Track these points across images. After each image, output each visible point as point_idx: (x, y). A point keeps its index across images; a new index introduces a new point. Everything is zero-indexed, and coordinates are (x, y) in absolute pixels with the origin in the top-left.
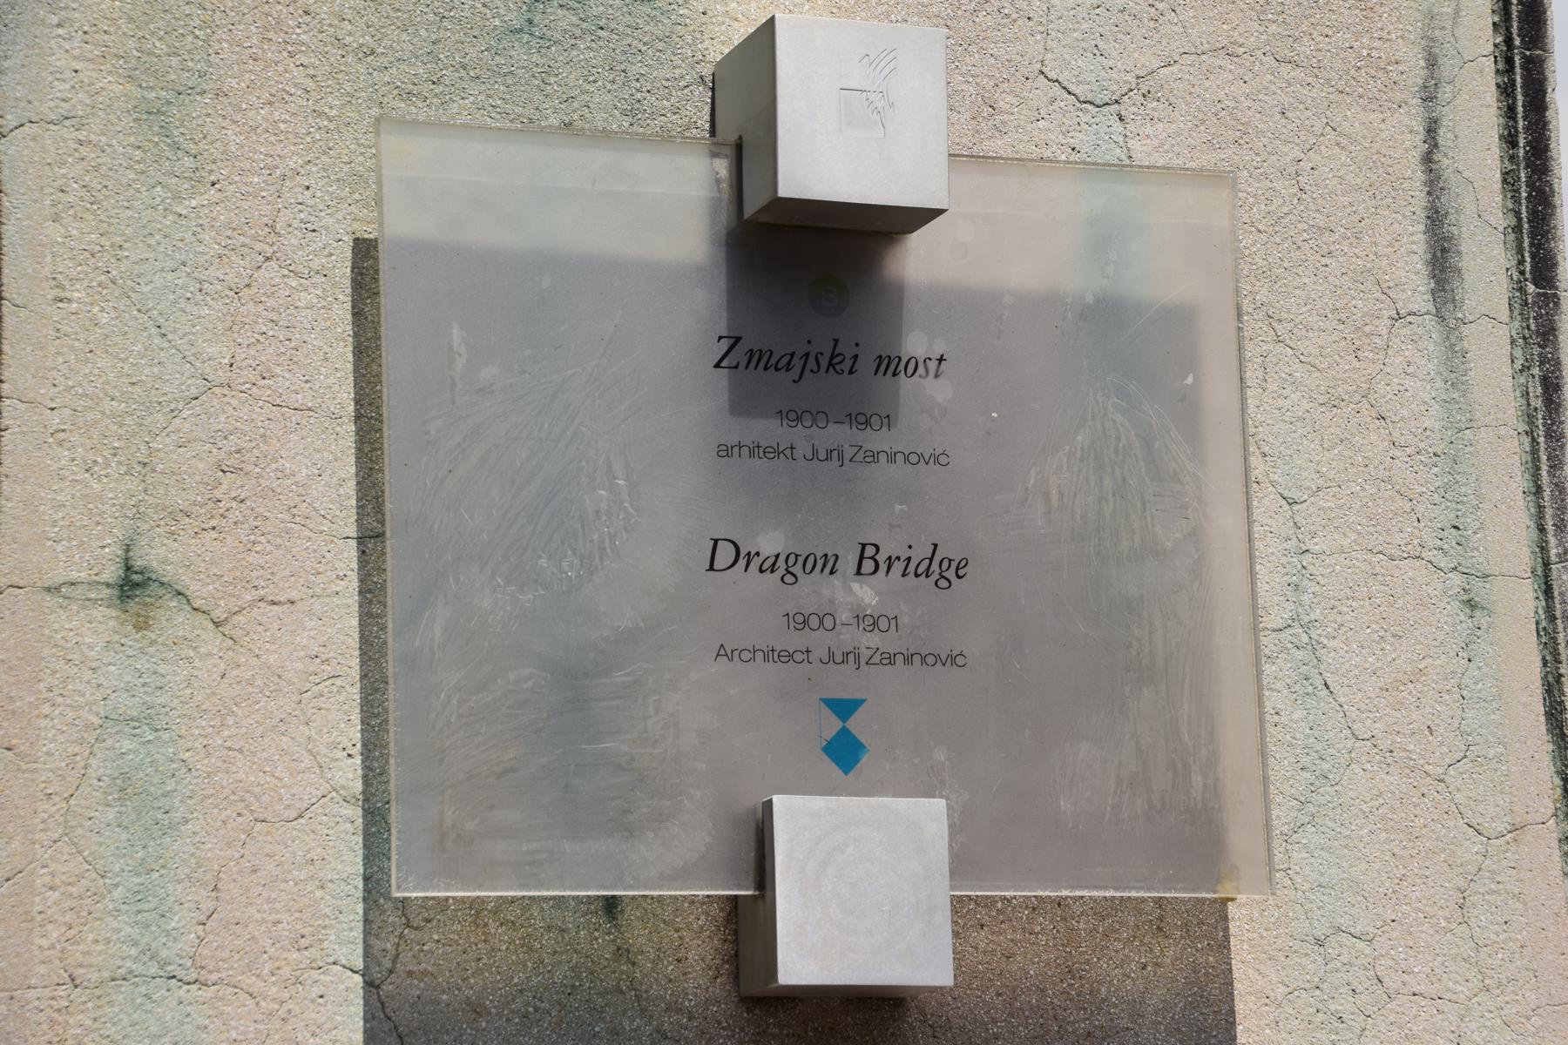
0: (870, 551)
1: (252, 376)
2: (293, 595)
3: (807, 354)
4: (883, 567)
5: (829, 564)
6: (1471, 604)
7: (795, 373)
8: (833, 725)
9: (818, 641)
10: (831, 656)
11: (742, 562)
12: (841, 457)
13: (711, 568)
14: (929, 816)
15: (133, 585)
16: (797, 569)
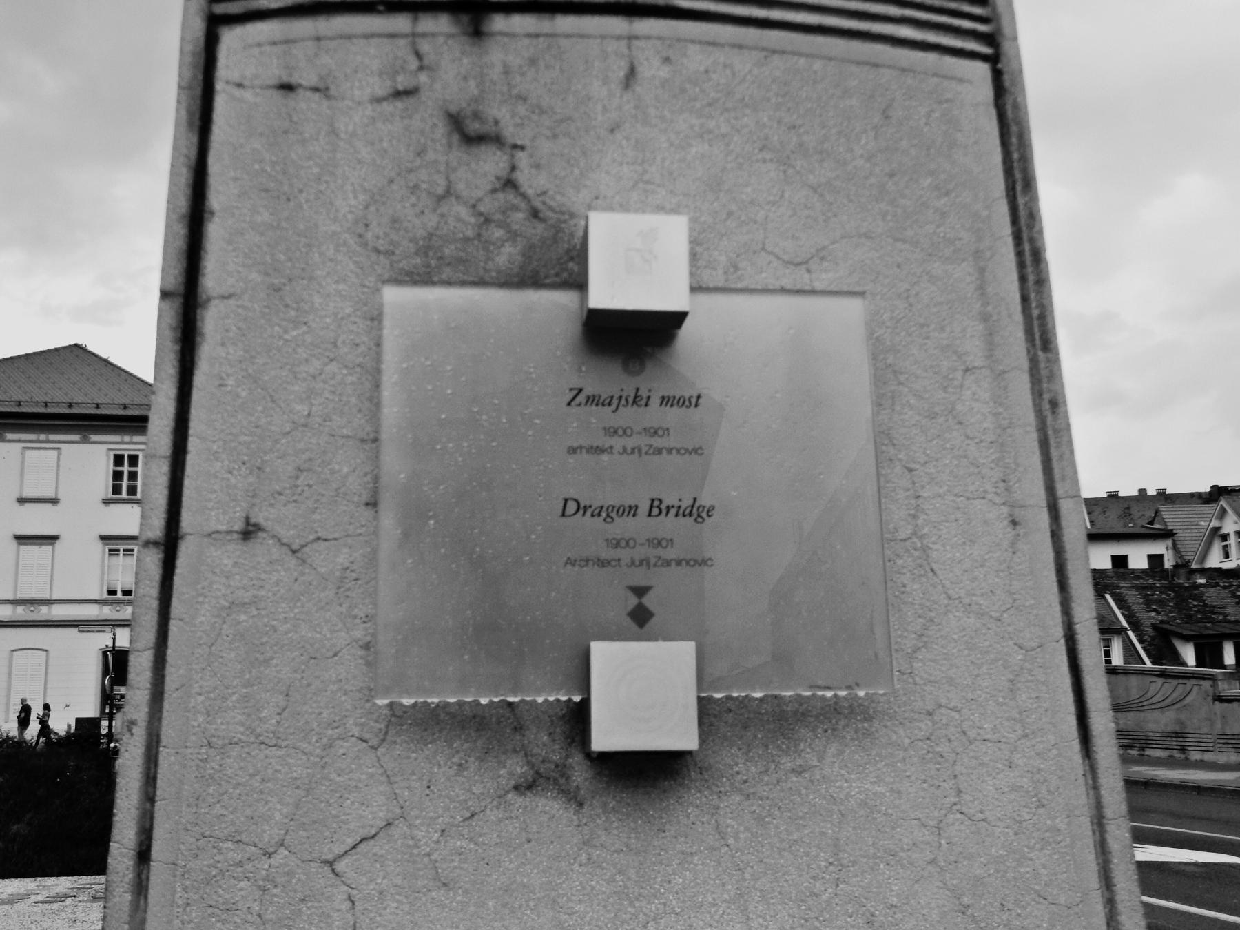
0: (656, 503)
1: (318, 420)
2: (336, 535)
3: (621, 397)
4: (664, 512)
5: (632, 510)
6: (1014, 523)
7: (614, 407)
8: (633, 601)
9: (624, 554)
10: (633, 563)
11: (581, 512)
12: (640, 451)
13: (563, 515)
14: (685, 651)
15: (249, 531)
16: (614, 515)
